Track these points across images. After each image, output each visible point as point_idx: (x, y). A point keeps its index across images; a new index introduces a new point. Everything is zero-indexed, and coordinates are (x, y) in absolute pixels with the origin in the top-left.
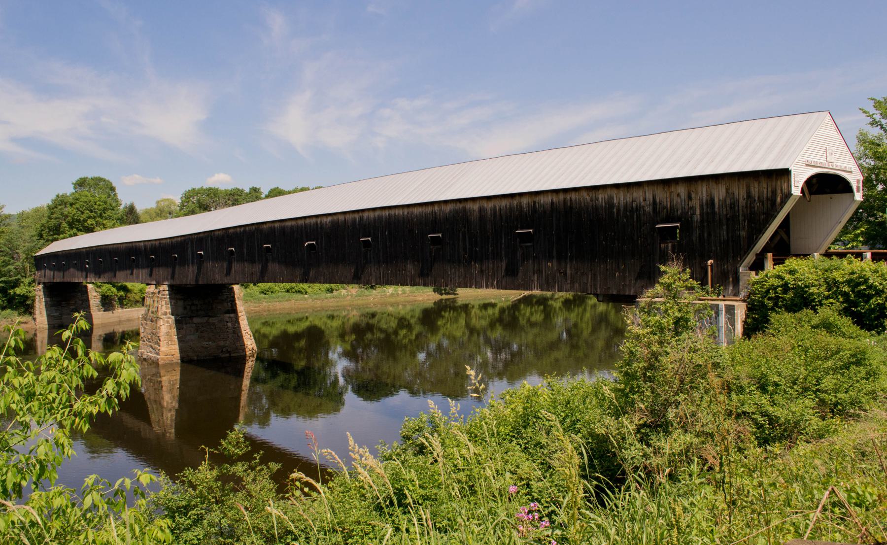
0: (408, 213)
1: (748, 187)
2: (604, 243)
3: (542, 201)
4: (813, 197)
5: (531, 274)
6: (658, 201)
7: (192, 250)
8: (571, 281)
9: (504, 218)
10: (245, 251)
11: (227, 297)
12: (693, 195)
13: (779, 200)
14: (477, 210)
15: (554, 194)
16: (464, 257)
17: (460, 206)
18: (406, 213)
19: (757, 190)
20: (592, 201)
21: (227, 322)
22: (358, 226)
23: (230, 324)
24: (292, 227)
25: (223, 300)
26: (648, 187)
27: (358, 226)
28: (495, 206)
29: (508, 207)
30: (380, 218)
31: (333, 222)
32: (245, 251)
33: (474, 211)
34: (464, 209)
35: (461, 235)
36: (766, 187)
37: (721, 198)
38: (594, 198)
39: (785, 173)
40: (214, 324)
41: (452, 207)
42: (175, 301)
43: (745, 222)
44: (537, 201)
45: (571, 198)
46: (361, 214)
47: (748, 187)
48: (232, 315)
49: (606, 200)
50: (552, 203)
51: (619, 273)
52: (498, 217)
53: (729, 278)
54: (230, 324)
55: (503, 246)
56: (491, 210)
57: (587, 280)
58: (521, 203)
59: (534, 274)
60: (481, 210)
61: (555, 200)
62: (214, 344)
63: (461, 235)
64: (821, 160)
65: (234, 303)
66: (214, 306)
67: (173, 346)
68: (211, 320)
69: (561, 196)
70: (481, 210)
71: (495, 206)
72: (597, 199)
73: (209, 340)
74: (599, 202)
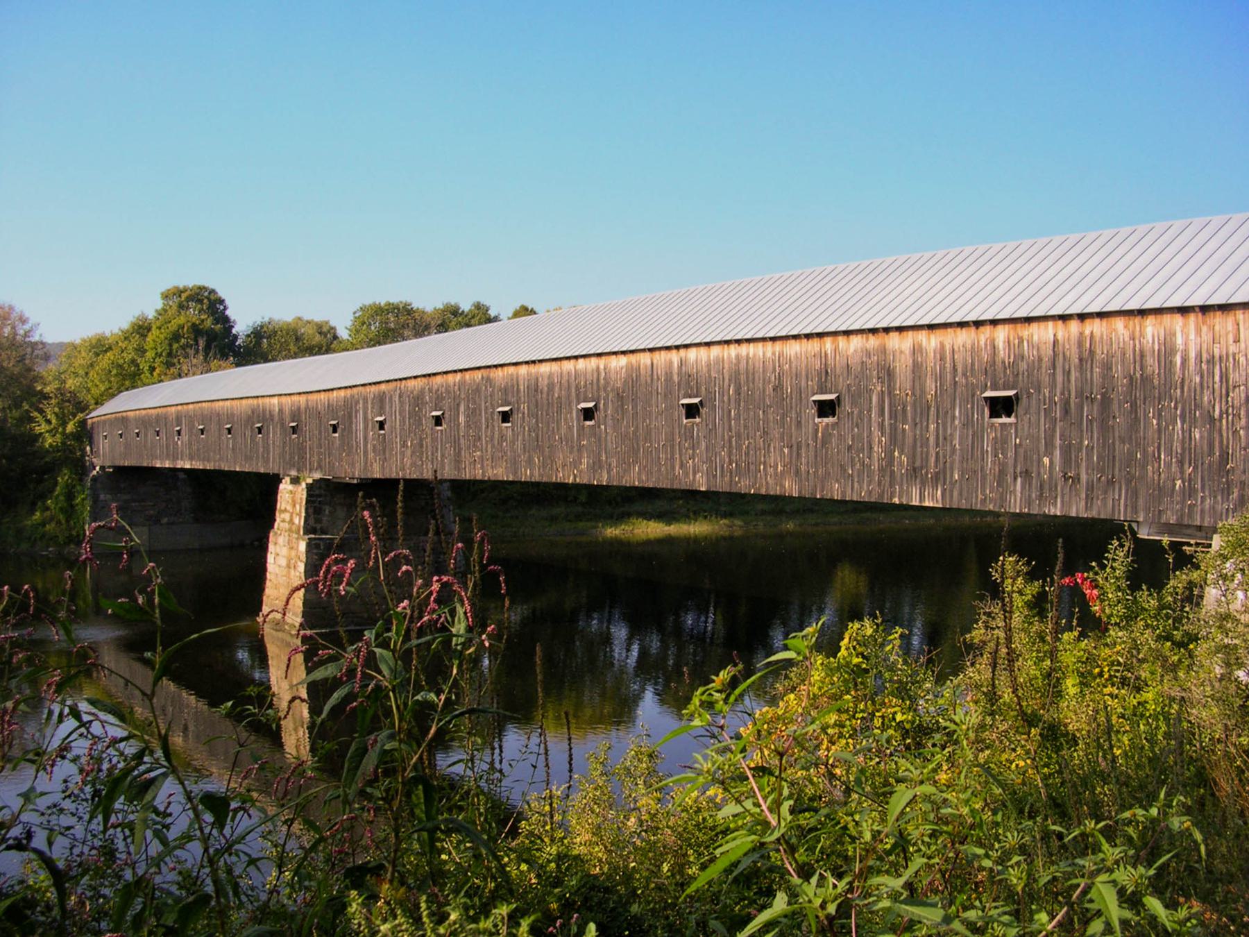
0: (774, 354)
2: (1155, 422)
3: (1035, 338)
5: (1010, 479)
7: (365, 414)
8: (1087, 496)
9: (960, 370)
10: (462, 419)
14: (907, 352)
15: (1060, 322)
17: (873, 342)
18: (769, 354)
20: (1134, 339)
22: (676, 378)
24: (550, 376)
27: (676, 378)
28: (942, 346)
29: (969, 347)
30: (720, 361)
31: (630, 367)
32: (462, 419)
33: (901, 352)
34: (883, 350)
35: (875, 399)
38: (1137, 334)
41: (860, 345)
44: (1025, 337)
45: (1092, 333)
46: (682, 352)
49: (1162, 338)
50: (1055, 342)
52: (948, 365)
55: (957, 422)
56: (935, 353)
58: (993, 341)
59: (1015, 479)
60: (916, 350)
61: (1060, 336)
63: (875, 399)
69: (1074, 326)
70: (916, 350)
71: (942, 346)
72: (1142, 335)
74: (1148, 342)
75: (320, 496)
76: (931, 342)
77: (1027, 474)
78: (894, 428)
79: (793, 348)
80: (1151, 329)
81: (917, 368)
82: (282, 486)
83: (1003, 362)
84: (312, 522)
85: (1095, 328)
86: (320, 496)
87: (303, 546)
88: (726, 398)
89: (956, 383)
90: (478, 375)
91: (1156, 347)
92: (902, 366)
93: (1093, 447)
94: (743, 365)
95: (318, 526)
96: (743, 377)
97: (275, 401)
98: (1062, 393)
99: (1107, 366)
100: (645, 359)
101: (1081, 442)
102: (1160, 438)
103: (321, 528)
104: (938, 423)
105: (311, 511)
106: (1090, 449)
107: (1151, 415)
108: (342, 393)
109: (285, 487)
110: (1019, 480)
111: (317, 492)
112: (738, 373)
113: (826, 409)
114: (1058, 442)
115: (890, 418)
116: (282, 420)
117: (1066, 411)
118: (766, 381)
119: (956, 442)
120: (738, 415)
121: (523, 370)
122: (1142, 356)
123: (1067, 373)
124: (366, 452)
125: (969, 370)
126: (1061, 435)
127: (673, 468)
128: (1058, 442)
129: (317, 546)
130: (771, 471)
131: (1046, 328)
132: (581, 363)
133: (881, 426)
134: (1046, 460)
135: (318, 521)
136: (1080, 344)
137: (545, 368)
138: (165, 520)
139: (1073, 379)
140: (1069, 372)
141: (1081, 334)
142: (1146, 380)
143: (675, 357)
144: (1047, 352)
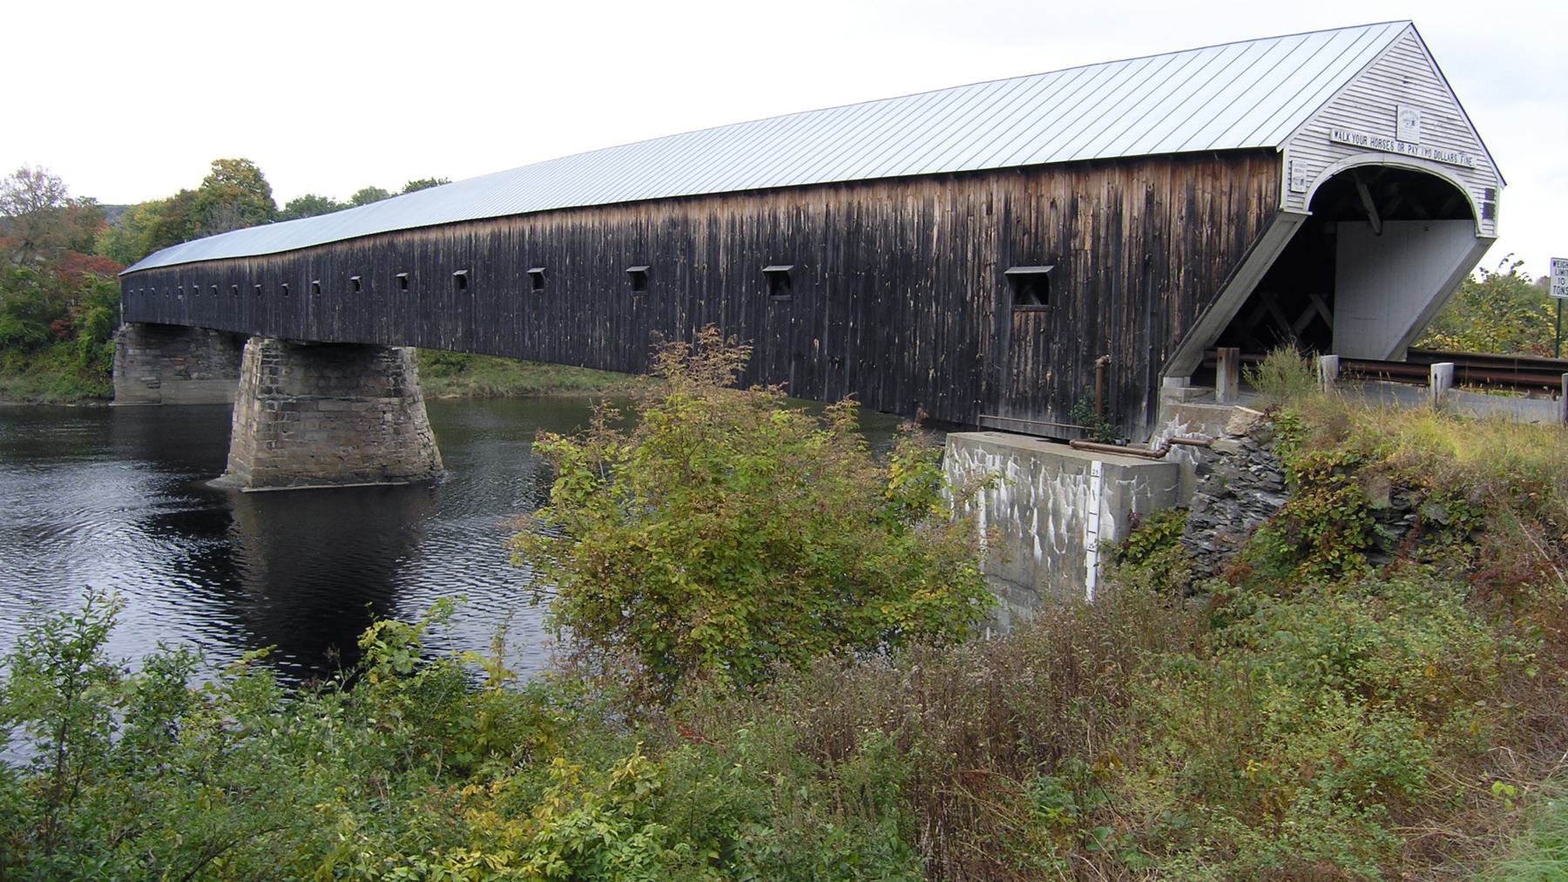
1: (1192, 190)
4: (1387, 223)
5: (786, 363)
6: (1013, 215)
11: (388, 367)
12: (1081, 205)
13: (1252, 220)
15: (832, 192)
16: (681, 317)
17: (678, 213)
19: (1208, 197)
21: (384, 412)
23: (389, 417)
24: (436, 243)
25: (379, 372)
26: (997, 182)
27: (527, 247)
36: (1226, 189)
37: (1136, 214)
39: (1268, 157)
40: (358, 415)
42: (289, 371)
43: (1179, 272)
45: (859, 203)
47: (1192, 190)
48: (395, 400)
49: (921, 209)
50: (828, 213)
51: (936, 372)
53: (1141, 400)
54: (389, 417)
56: (727, 224)
57: (879, 384)
62: (356, 451)
64: (1385, 135)
65: (400, 379)
66: (362, 383)
67: (279, 451)
68: (355, 407)
69: (844, 197)
73: (349, 442)
75: (276, 357)
76: (724, 214)
77: (799, 356)
78: (691, 301)
79: (615, 219)
80: (912, 204)
81: (712, 239)
82: (246, 346)
83: (783, 234)
84: (268, 383)
85: (863, 198)
86: (276, 357)
87: (257, 406)
88: (563, 269)
89: (743, 255)
90: (385, 240)
91: (916, 221)
92: (701, 236)
93: (857, 329)
94: (576, 237)
95: (274, 386)
96: (576, 246)
97: (247, 263)
98: (832, 270)
99: (871, 241)
100: (504, 228)
101: (848, 324)
102: (916, 322)
103: (277, 388)
104: (728, 300)
105: (267, 371)
106: (855, 330)
107: (909, 295)
108: (291, 257)
109: (249, 347)
110: (793, 363)
111: (273, 353)
112: (573, 243)
113: (639, 280)
114: (827, 323)
115: (690, 293)
116: (251, 284)
117: (834, 290)
118: (595, 251)
119: (742, 319)
120: (573, 286)
121: (417, 237)
122: (903, 229)
123: (836, 248)
124: (307, 315)
125: (756, 244)
126: (830, 316)
127: (524, 340)
128: (827, 323)
129: (271, 406)
130: (596, 345)
131: (821, 196)
132: (449, 233)
133: (683, 301)
134: (817, 343)
135: (274, 381)
136: (849, 216)
137: (432, 236)
138: (195, 375)
139: (842, 253)
140: (838, 246)
141: (850, 204)
142: (907, 256)
143: (526, 226)
144: (821, 222)
